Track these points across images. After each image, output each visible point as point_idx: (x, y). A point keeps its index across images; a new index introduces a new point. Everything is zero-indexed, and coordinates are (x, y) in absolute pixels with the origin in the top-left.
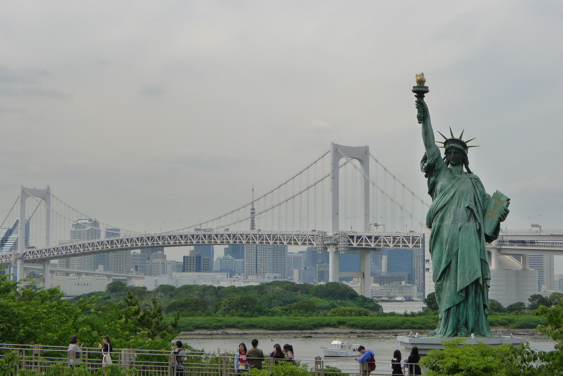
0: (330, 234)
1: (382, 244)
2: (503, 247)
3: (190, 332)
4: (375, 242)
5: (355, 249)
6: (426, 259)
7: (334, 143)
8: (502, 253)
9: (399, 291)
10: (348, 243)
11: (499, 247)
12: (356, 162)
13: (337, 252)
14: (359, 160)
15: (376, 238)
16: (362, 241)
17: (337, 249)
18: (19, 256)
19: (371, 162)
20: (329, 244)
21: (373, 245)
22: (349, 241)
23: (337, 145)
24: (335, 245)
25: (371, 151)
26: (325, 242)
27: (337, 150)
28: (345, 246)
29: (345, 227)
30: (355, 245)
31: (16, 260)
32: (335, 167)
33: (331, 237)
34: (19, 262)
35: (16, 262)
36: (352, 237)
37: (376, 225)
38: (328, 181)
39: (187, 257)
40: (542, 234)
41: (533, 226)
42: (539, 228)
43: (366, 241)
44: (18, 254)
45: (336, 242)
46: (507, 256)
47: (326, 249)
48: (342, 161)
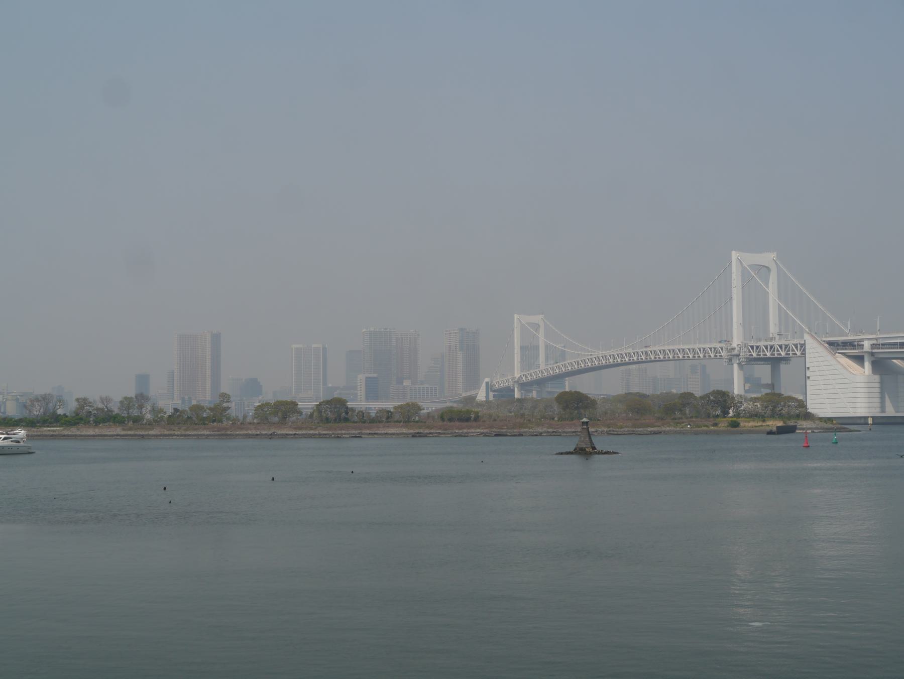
5: (755, 359)
6: (807, 366)
8: (876, 356)
10: (749, 354)
13: (739, 364)
16: (774, 351)
17: (739, 359)
21: (768, 354)
22: (750, 352)
24: (738, 355)
27: (738, 258)
28: (746, 356)
30: (754, 355)
33: (733, 349)
36: (752, 347)
45: (738, 353)
46: (895, 361)
47: (731, 361)
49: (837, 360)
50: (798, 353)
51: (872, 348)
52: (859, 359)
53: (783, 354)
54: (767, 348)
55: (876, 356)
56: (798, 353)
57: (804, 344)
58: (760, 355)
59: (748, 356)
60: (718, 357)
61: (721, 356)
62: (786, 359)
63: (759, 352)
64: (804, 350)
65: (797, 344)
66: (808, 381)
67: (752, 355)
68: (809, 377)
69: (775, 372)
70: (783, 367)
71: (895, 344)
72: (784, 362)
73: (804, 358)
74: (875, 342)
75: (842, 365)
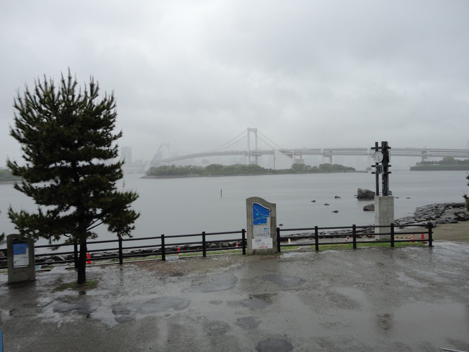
0: (248, 151)
1: (262, 154)
5: (255, 155)
6: (275, 157)
12: (254, 132)
14: (255, 132)
15: (260, 152)
16: (256, 153)
17: (250, 155)
19: (258, 132)
20: (247, 154)
21: (260, 154)
25: (258, 129)
26: (247, 154)
30: (255, 154)
32: (249, 134)
36: (254, 152)
37: (260, 149)
38: (247, 137)
41: (304, 147)
42: (305, 148)
48: (251, 132)
52: (291, 156)
66: (275, 161)
68: (275, 160)
70: (259, 157)
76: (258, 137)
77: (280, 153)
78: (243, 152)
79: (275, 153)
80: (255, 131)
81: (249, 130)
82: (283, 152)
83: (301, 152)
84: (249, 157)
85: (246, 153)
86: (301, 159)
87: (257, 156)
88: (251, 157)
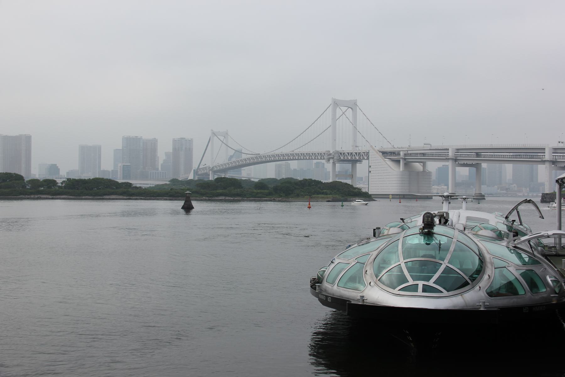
2: (406, 157)
3: (15, 197)
4: (350, 156)
7: (333, 98)
9: (465, 191)
11: (403, 157)
14: (351, 108)
17: (333, 160)
18: (211, 169)
21: (349, 158)
23: (335, 99)
29: (339, 149)
30: (342, 158)
31: (210, 170)
33: (331, 154)
34: (210, 172)
35: (209, 172)
36: (341, 153)
39: (340, 172)
40: (432, 148)
43: (347, 156)
44: (210, 167)
45: (333, 157)
49: (386, 162)
50: (366, 158)
51: (405, 156)
52: (398, 162)
53: (357, 158)
54: (349, 154)
55: (407, 160)
56: (366, 158)
57: (369, 153)
58: (345, 158)
59: (338, 159)
60: (311, 158)
61: (324, 158)
62: (360, 161)
63: (344, 156)
64: (368, 156)
65: (365, 153)
67: (341, 158)
68: (370, 171)
69: (354, 167)
70: (358, 165)
71: (417, 154)
72: (359, 163)
73: (368, 160)
74: (406, 152)
75: (388, 165)
76: (351, 120)
77: (379, 157)
78: (324, 153)
79: (370, 157)
80: (353, 106)
81: (336, 104)
82: (384, 153)
83: (424, 154)
84: (334, 164)
85: (329, 157)
86: (424, 171)
87: (354, 162)
88: (338, 165)
